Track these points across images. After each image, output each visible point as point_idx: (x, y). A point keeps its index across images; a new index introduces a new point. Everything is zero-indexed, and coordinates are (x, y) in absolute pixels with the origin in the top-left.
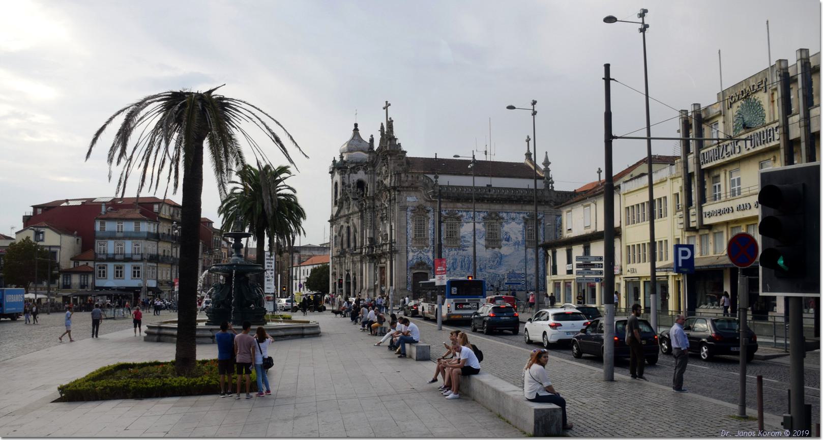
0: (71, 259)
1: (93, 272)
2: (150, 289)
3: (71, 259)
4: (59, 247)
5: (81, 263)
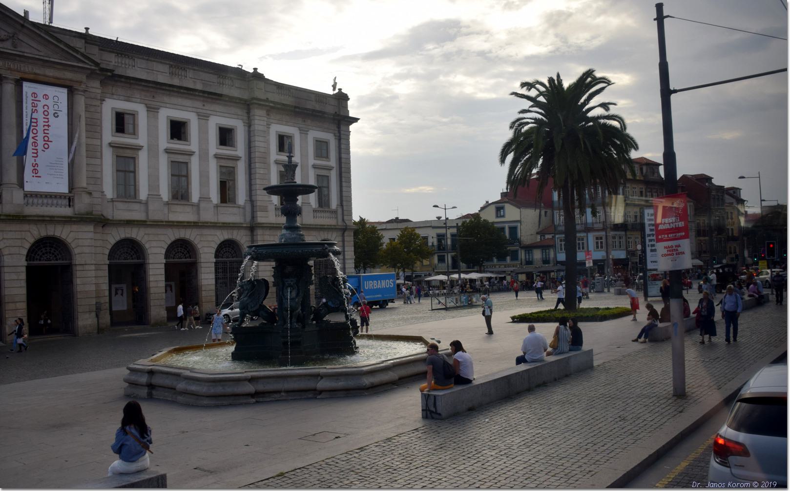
0: (537, 233)
1: (553, 246)
2: (617, 262)
3: (537, 233)
4: (520, 221)
5: (547, 236)
